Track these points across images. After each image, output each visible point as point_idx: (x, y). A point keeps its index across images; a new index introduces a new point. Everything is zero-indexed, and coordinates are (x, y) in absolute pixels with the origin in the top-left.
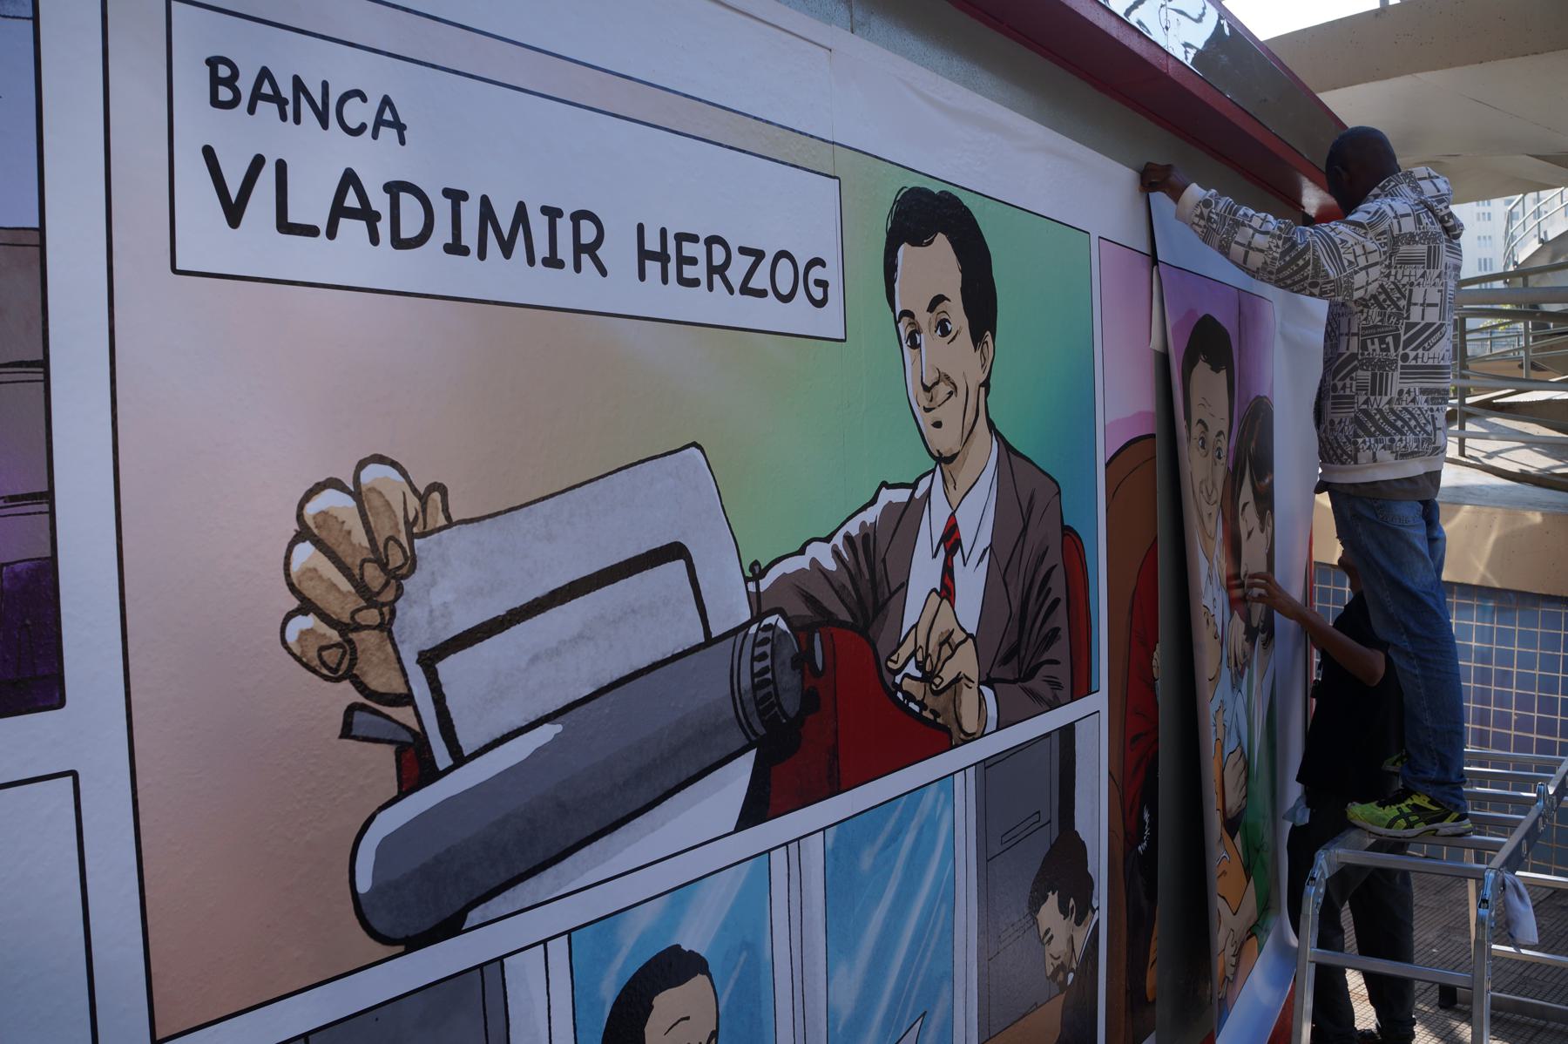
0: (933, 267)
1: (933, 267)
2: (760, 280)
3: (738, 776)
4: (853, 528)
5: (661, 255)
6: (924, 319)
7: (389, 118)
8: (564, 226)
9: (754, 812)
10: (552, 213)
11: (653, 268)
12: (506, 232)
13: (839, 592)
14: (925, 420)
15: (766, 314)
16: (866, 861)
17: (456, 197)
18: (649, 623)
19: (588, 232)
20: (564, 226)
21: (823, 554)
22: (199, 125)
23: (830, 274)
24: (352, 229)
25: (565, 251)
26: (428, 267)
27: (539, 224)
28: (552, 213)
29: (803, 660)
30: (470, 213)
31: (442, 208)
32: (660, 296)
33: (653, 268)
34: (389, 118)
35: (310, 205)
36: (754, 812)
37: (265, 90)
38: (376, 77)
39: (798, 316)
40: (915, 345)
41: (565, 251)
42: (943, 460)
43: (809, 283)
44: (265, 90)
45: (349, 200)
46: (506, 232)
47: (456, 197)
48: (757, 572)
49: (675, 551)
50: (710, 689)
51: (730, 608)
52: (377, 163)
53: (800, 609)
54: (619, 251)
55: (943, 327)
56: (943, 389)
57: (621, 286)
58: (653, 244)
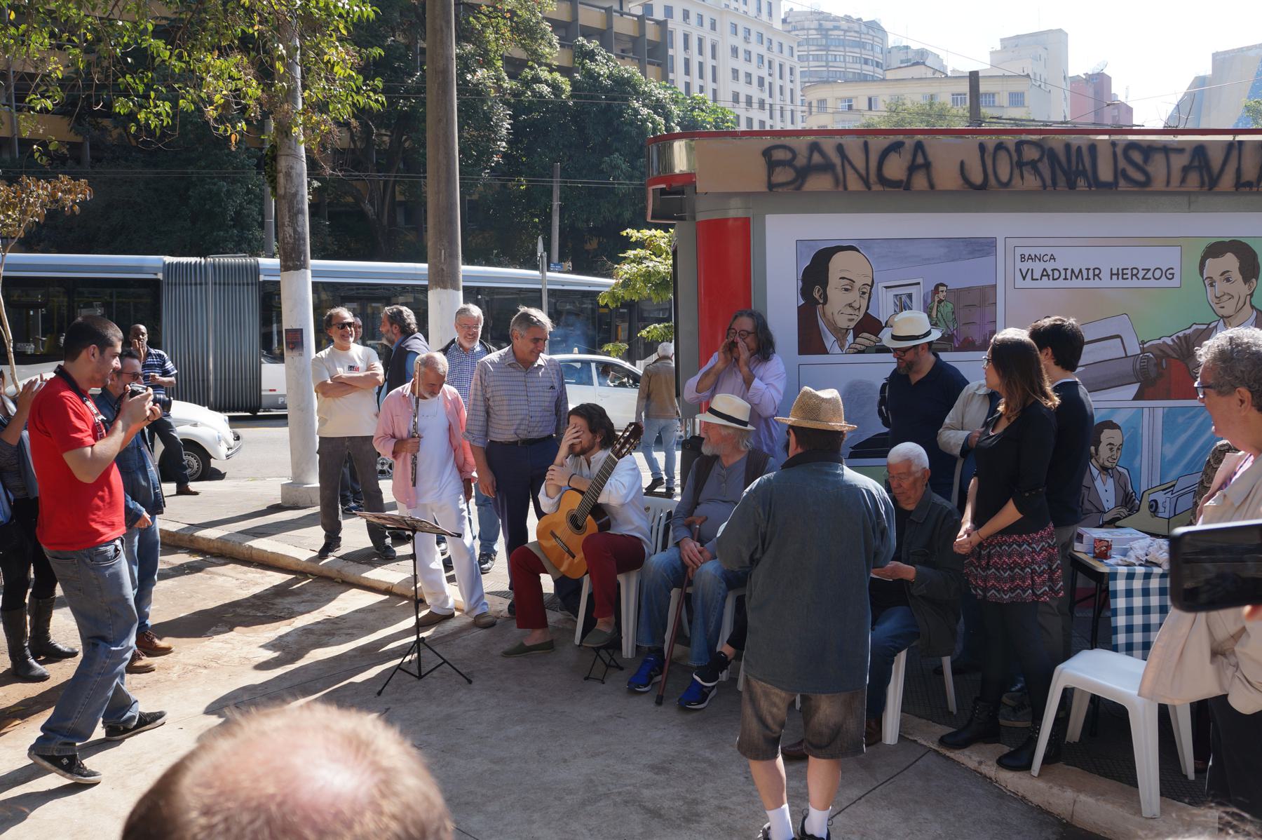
0: (1230, 262)
1: (1230, 262)
2: (1149, 275)
3: (1134, 388)
4: (1181, 334)
5: (1119, 274)
6: (1216, 277)
7: (1053, 258)
8: (1091, 272)
9: (1138, 397)
10: (1088, 269)
11: (1115, 277)
12: (1077, 274)
13: (1173, 350)
14: (1216, 307)
15: (1152, 283)
16: (1180, 420)
17: (1066, 270)
18: (1112, 350)
19: (1097, 272)
20: (1091, 272)
21: (1169, 341)
22: (1019, 265)
23: (1177, 272)
24: (1045, 278)
25: (1091, 276)
26: (1061, 283)
27: (1085, 273)
28: (1088, 269)
29: (1158, 365)
30: (1069, 272)
31: (1063, 273)
32: (1116, 282)
33: (1115, 277)
34: (1053, 258)
35: (1037, 275)
36: (1138, 397)
37: (1030, 257)
38: (1049, 251)
39: (1164, 282)
40: (1211, 285)
41: (1091, 276)
42: (1223, 317)
43: (1168, 274)
44: (1030, 257)
45: (1044, 273)
46: (1077, 274)
47: (1066, 270)
48: (1143, 343)
49: (1118, 336)
50: (1127, 366)
51: (1134, 349)
52: (1050, 266)
53: (1158, 352)
54: (1105, 274)
55: (1228, 280)
56: (1226, 297)
57: (1106, 281)
58: (1115, 271)
